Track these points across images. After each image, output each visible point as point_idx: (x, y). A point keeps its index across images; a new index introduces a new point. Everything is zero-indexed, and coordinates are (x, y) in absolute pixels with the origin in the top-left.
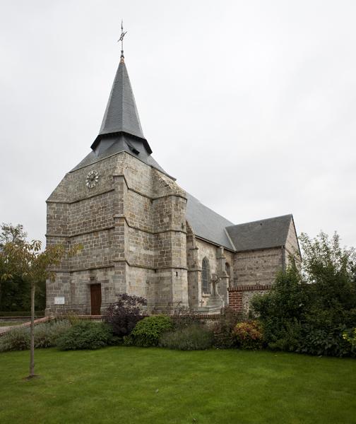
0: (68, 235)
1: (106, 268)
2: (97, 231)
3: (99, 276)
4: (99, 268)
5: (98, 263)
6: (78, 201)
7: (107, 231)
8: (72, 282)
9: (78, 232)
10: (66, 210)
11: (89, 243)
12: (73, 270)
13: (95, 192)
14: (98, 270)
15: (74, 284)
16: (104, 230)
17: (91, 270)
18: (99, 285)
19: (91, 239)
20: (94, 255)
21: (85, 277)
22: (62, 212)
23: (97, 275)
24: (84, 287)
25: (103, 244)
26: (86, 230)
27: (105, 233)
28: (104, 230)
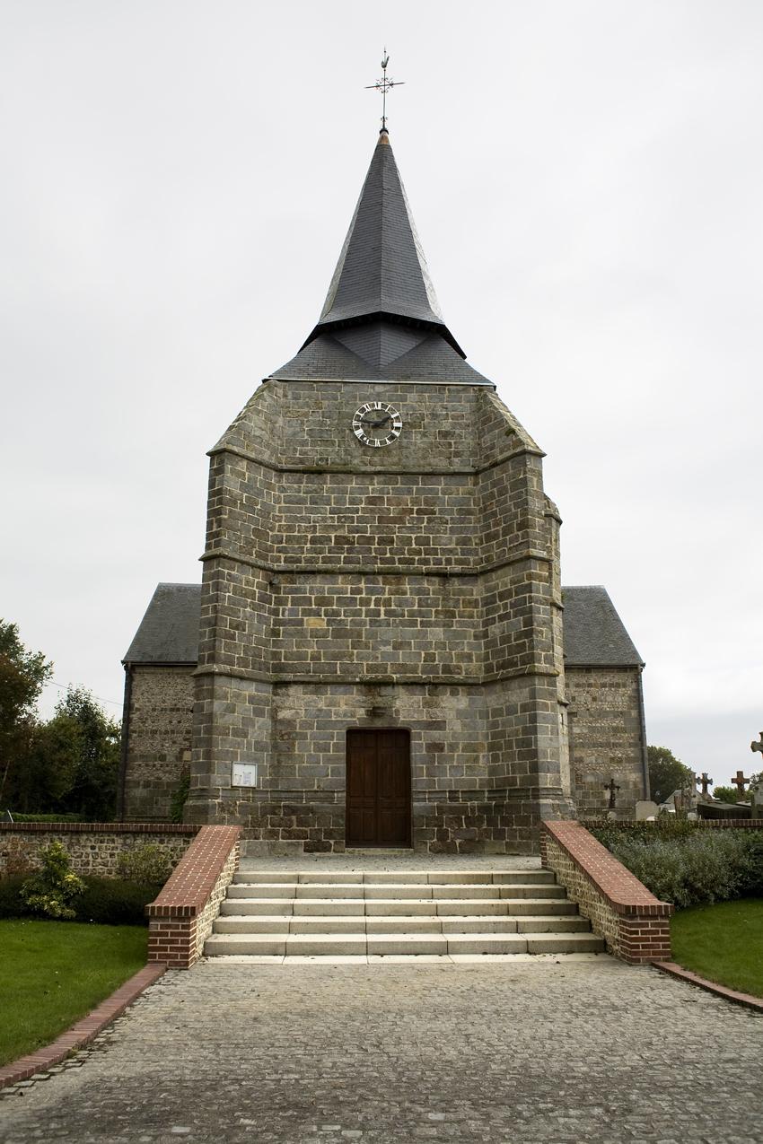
0: (269, 564)
1: (436, 685)
2: (398, 575)
3: (406, 707)
4: (405, 684)
5: (402, 668)
6: (320, 472)
7: (436, 579)
8: (283, 714)
9: (314, 560)
10: (269, 486)
11: (366, 602)
12: (290, 677)
13: (390, 463)
14: (400, 690)
15: (290, 723)
16: (429, 574)
17: (371, 686)
18: (404, 735)
19: (371, 591)
20: (386, 643)
21: (348, 708)
22: (260, 494)
23: (398, 704)
24: (338, 738)
25: (421, 614)
26: (347, 561)
27: (431, 586)
28: (429, 574)
